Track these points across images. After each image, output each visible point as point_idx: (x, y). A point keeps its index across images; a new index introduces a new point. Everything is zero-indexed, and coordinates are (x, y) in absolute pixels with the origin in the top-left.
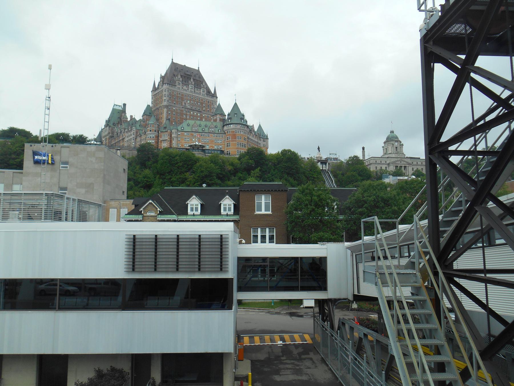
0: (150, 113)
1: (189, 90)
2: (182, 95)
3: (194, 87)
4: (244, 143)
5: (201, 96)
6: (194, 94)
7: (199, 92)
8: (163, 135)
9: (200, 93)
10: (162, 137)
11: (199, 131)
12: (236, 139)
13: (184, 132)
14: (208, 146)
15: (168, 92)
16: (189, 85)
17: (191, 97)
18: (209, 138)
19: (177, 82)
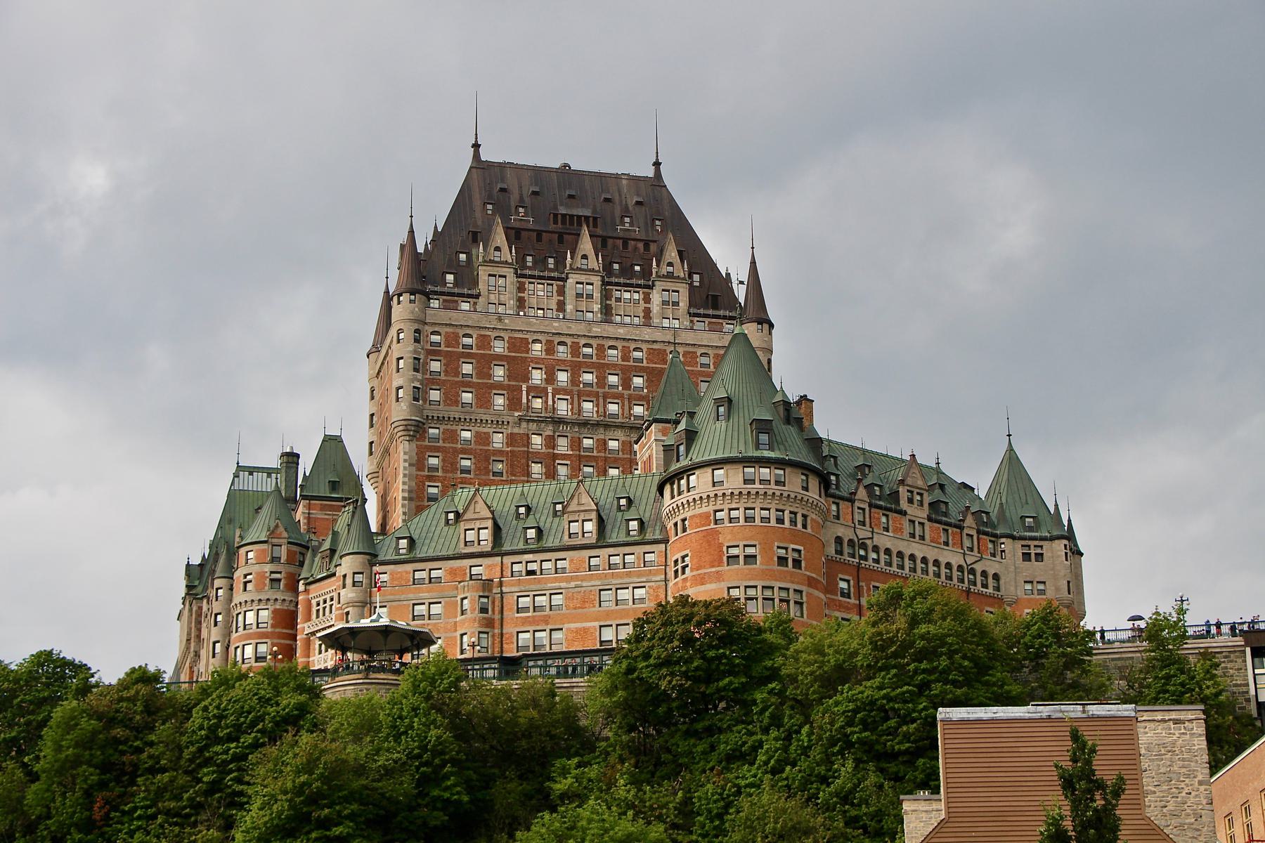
0: (334, 486)
2: (519, 345)
3: (604, 283)
4: (792, 586)
5: (647, 334)
6: (596, 330)
8: (318, 604)
9: (647, 312)
10: (314, 616)
11: (506, 547)
12: (720, 563)
13: (410, 567)
15: (417, 341)
16: (565, 280)
18: (561, 580)
19: (483, 273)
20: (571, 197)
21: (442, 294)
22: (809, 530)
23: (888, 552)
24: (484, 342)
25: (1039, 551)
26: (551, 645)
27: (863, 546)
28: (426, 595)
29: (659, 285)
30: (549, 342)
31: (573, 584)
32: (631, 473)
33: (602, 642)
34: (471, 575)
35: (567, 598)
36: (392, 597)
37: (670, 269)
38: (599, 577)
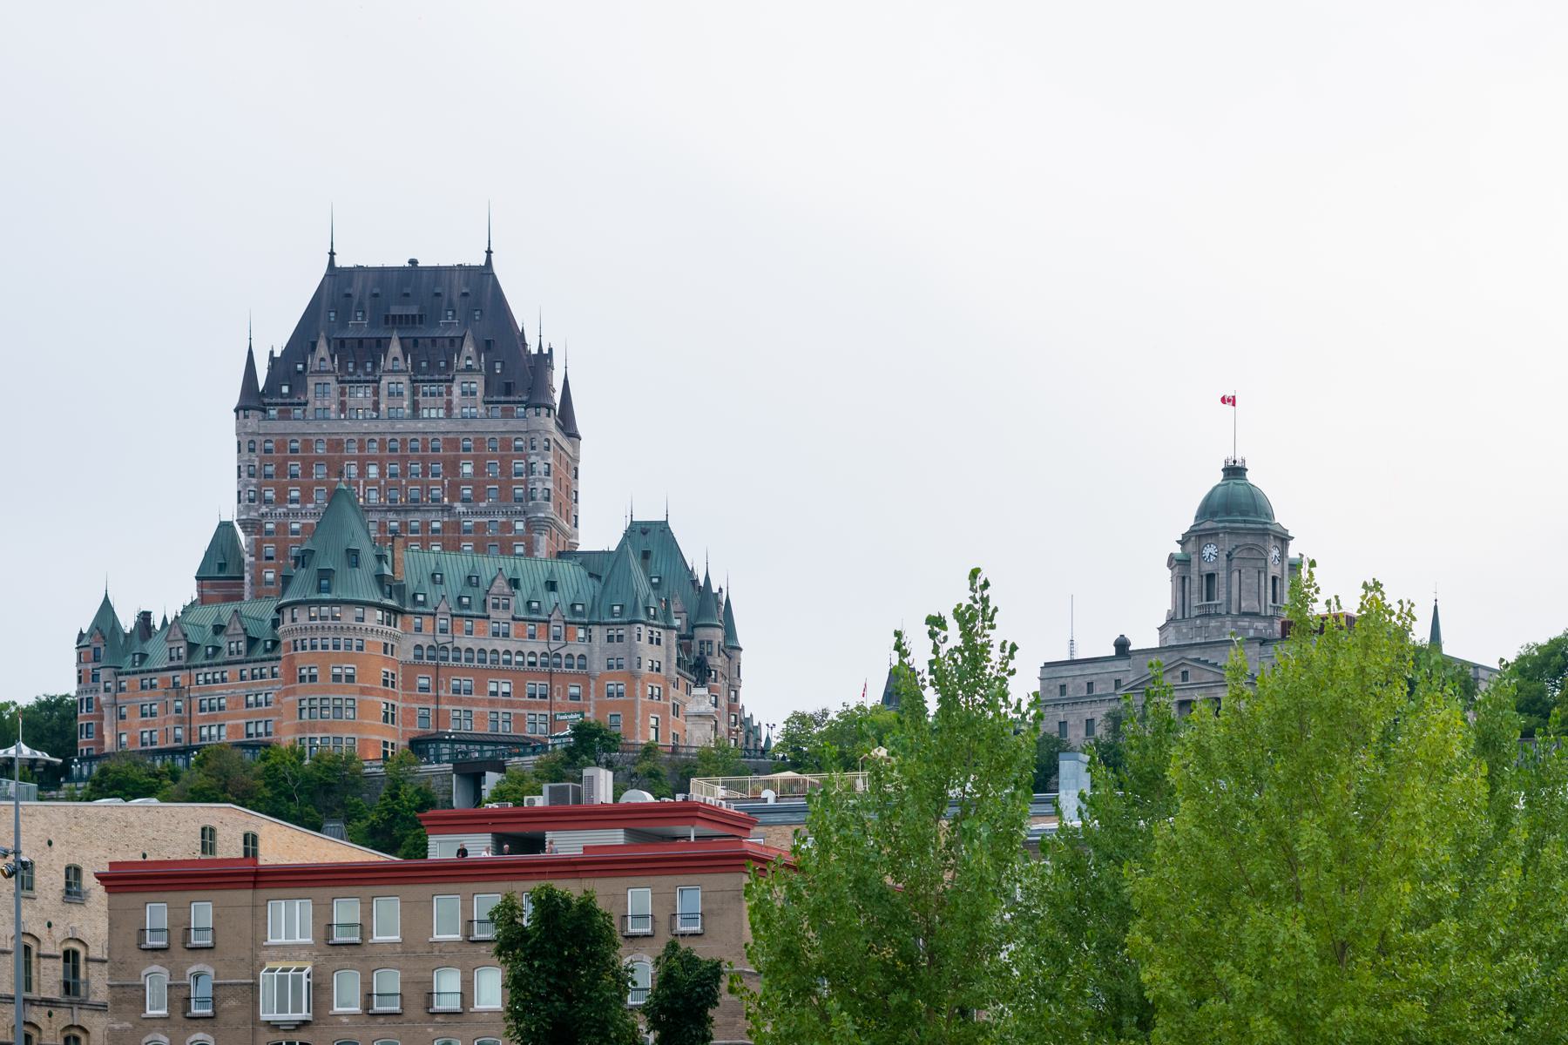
1: (382, 406)
2: (335, 445)
3: (413, 382)
7: (441, 401)
9: (449, 403)
12: (295, 682)
13: (138, 677)
14: (223, 731)
16: (378, 382)
17: (382, 440)
20: (407, 295)
21: (277, 404)
22: (365, 651)
23: (469, 650)
24: (307, 445)
25: (620, 632)
26: (219, 736)
27: (445, 649)
28: (147, 698)
29: (458, 379)
30: (361, 441)
31: (230, 691)
32: (428, 549)
33: (249, 735)
34: (174, 683)
35: (227, 701)
36: (127, 700)
37: (469, 362)
38: (244, 686)
